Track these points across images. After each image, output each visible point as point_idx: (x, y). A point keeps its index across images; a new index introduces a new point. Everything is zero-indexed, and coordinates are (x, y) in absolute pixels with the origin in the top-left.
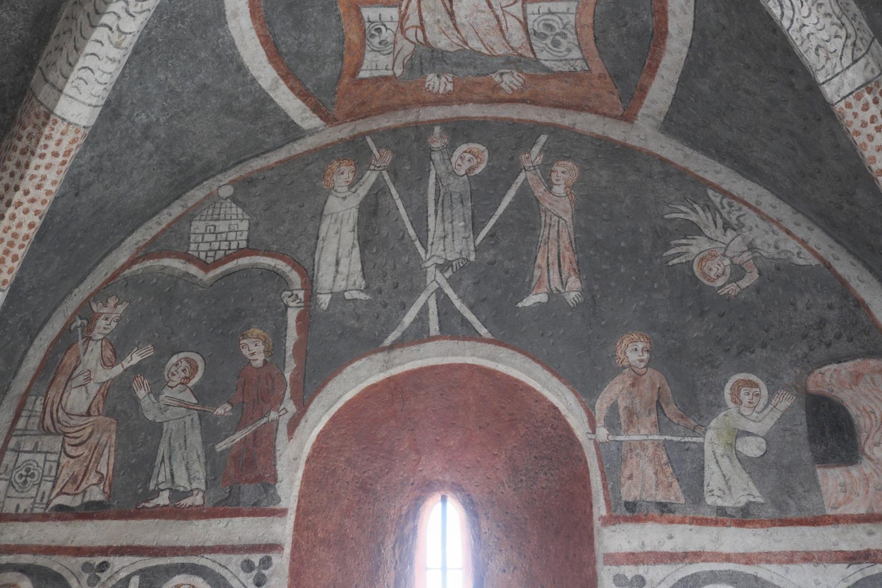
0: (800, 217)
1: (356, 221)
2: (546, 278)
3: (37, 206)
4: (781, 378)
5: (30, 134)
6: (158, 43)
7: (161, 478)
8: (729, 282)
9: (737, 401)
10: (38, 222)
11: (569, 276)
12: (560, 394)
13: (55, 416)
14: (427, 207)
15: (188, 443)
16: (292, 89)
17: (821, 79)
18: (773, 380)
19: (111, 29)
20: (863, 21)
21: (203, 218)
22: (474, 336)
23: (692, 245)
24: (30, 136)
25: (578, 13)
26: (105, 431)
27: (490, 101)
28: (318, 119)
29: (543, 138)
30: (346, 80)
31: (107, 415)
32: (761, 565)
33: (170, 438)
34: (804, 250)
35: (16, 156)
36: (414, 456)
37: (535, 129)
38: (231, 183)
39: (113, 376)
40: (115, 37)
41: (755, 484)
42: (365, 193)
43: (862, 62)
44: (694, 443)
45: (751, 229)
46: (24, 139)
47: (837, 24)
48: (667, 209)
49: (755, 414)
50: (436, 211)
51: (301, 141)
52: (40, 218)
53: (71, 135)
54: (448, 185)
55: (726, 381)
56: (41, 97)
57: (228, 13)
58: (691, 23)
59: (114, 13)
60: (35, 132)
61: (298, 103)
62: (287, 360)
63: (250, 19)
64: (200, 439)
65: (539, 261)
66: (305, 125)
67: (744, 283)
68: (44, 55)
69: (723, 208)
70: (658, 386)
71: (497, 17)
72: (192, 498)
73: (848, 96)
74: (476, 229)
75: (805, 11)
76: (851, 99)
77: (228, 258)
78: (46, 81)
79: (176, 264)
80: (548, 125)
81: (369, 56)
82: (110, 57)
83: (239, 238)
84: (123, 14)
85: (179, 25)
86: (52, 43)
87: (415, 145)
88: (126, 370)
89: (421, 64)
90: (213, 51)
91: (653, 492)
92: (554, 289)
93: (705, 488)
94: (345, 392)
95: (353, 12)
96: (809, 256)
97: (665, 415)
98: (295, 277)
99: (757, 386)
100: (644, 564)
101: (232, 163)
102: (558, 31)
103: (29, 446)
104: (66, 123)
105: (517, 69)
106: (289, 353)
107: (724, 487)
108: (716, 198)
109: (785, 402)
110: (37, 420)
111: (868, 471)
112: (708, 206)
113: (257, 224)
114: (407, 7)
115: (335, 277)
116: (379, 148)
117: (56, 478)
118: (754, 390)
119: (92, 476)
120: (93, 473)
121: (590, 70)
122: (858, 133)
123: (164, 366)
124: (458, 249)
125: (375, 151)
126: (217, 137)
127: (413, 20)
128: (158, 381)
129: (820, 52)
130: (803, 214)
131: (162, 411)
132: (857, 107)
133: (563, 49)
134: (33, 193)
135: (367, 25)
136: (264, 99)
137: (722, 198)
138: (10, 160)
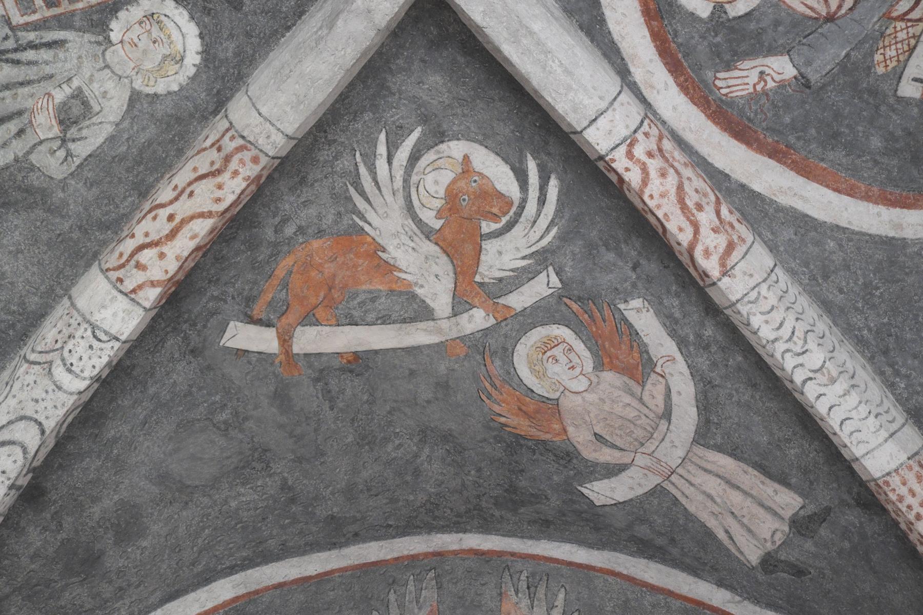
19: (810, 379)
40: (821, 378)
57: (892, 234)
59: (795, 367)
63: (912, 212)
82: (842, 393)
84: (800, 360)
104: (894, 474)
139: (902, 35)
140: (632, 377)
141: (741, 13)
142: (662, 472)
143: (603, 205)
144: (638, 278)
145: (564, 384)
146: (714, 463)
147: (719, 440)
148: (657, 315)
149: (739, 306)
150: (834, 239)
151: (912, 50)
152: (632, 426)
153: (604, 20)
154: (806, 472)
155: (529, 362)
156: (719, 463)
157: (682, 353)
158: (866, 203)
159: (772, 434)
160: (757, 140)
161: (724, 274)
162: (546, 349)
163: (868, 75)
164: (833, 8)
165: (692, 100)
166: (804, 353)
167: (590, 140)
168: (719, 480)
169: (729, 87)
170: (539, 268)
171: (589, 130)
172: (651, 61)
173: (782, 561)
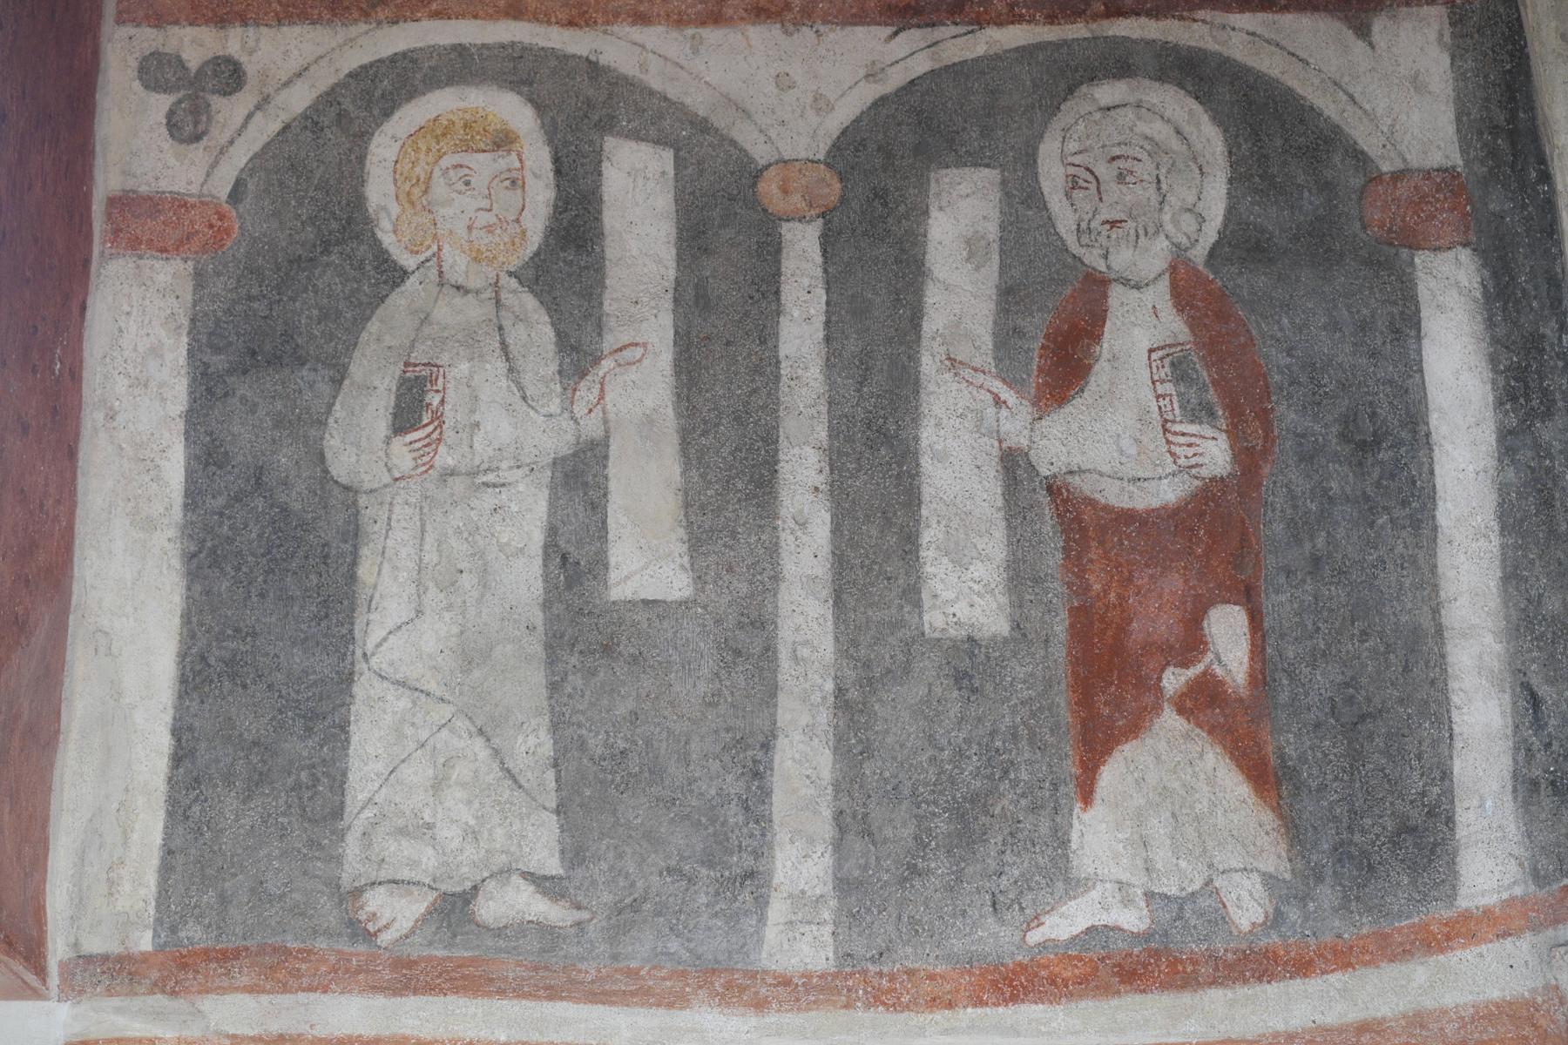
32: (616, 28)
100: (245, 24)
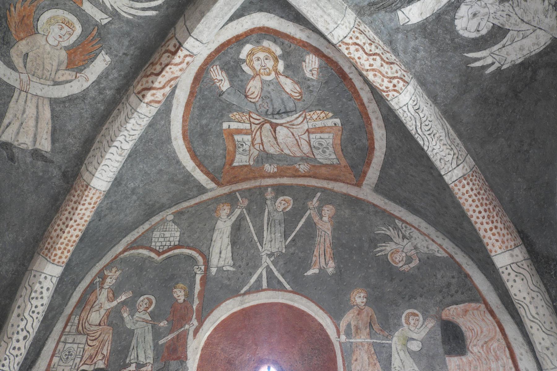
0: (439, 234)
1: (230, 232)
2: (318, 262)
3: (80, 227)
4: (429, 312)
5: (79, 194)
6: (140, 152)
7: (132, 357)
8: (405, 264)
9: (408, 323)
10: (80, 234)
11: (329, 260)
12: (324, 318)
13: (84, 326)
14: (263, 226)
15: (146, 340)
16: (202, 171)
17: (443, 173)
18: (425, 312)
19: (117, 148)
20: (463, 147)
21: (159, 230)
22: (284, 289)
23: (387, 246)
24: (78, 195)
25: (334, 138)
26: (107, 333)
27: (295, 176)
28: (214, 184)
29: (319, 194)
30: (227, 167)
31: (108, 326)
33: (137, 337)
34: (441, 250)
35: (72, 204)
36: (254, 347)
37: (315, 190)
38: (172, 214)
39: (113, 306)
40: (119, 151)
41: (416, 365)
42: (235, 219)
43: (461, 166)
44: (387, 343)
45: (415, 239)
46: (76, 196)
47: (449, 149)
48: (376, 229)
49: (416, 330)
50: (268, 228)
51: (206, 194)
52: (81, 233)
53: (97, 195)
54: (274, 216)
55: (403, 313)
56: (85, 178)
57: (172, 138)
58: (385, 145)
60: (81, 193)
61: (205, 177)
62: (195, 299)
64: (151, 338)
65: (315, 253)
66: (208, 187)
67: (412, 265)
68: (87, 158)
69: (402, 228)
70: (370, 315)
71: (296, 140)
72: (146, 367)
73: (455, 181)
74: (286, 237)
75: (434, 143)
76: (457, 182)
77: (169, 250)
78: (88, 170)
79: (145, 252)
80: (321, 188)
81: (238, 156)
83: (175, 240)
84: (123, 141)
85: (150, 144)
86: (91, 154)
87: (259, 196)
88: (119, 303)
89: (262, 160)
90: (166, 155)
91: (367, 368)
92: (322, 267)
93: (392, 366)
94: (221, 316)
95: (230, 137)
96: (443, 252)
97: (373, 329)
98: (200, 259)
99: (417, 315)
101: (173, 204)
102: (325, 146)
103: (70, 340)
105: (307, 162)
106: (196, 296)
107: (401, 366)
108: (399, 224)
109: (431, 324)
110: (75, 327)
111: (470, 359)
112: (396, 228)
113: (184, 233)
114: (255, 135)
115: (219, 260)
116: (242, 198)
117: (82, 357)
118: (416, 317)
119: (100, 355)
120: (100, 354)
121: (340, 164)
122: (461, 198)
123: (136, 302)
124: (277, 246)
125: (240, 199)
126: (167, 193)
127: (258, 140)
128: (134, 309)
129: (442, 161)
130: (440, 232)
131: (135, 324)
132: (460, 186)
133: (327, 154)
134: (79, 221)
135: (237, 143)
136: (189, 176)
137: (402, 224)
138: (69, 206)
139: (244, 118)
140: (68, 64)
141: (243, 68)
142: (23, 87)
143: (150, 35)
144: (120, 56)
145: (49, 34)
146: (44, 109)
147: (57, 109)
148: (106, 68)
149: (136, 113)
150: (165, 123)
151: (240, 122)
152: (41, 69)
153: (232, 21)
154: (65, 148)
155: (54, 17)
156: (44, 111)
157: (92, 83)
158: (181, 127)
159: (74, 130)
160: (196, 86)
161: (147, 104)
162: (66, 23)
163: (228, 112)
164: (250, 97)
165: (206, 59)
166: (127, 142)
167: (188, 39)
168: (35, 113)
169: (214, 71)
170: (109, 13)
171: (192, 39)
172: (219, 41)
173: (12, 151)
